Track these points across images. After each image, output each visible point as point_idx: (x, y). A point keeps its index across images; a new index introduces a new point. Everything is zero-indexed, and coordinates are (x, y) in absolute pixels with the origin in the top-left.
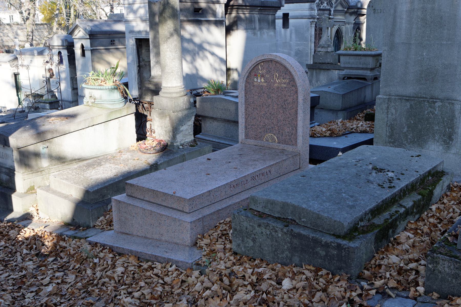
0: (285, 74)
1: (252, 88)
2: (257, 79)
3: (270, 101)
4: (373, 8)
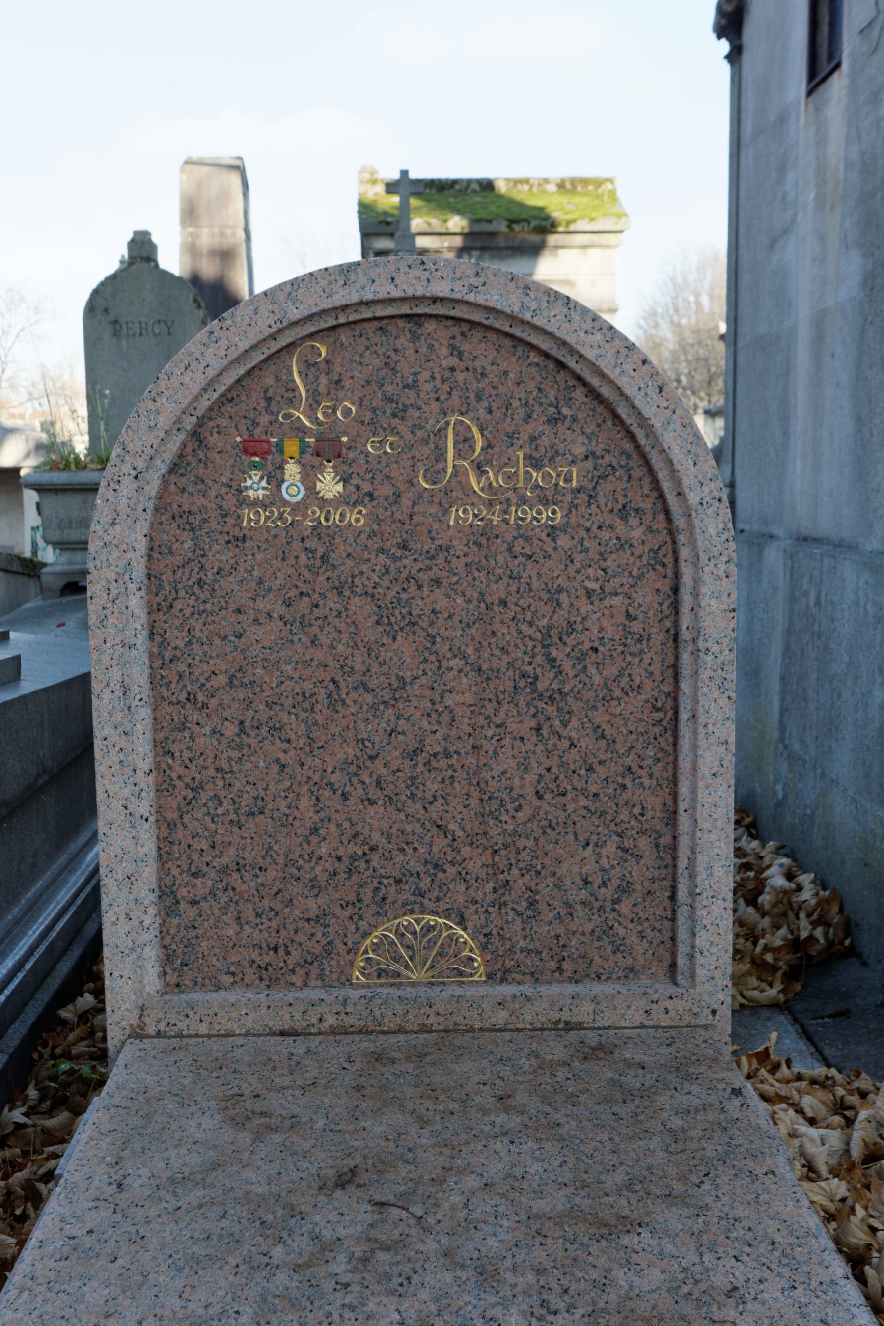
0: (553, 421)
1: (219, 555)
2: (276, 479)
3: (405, 650)
4: (111, 318)
